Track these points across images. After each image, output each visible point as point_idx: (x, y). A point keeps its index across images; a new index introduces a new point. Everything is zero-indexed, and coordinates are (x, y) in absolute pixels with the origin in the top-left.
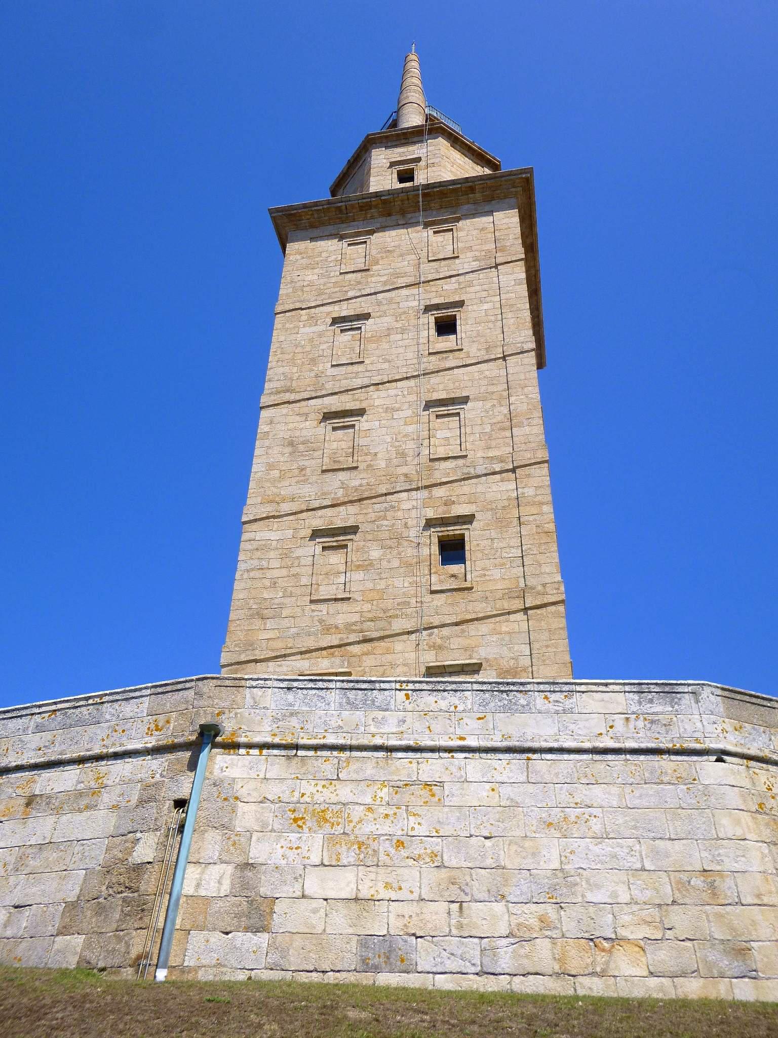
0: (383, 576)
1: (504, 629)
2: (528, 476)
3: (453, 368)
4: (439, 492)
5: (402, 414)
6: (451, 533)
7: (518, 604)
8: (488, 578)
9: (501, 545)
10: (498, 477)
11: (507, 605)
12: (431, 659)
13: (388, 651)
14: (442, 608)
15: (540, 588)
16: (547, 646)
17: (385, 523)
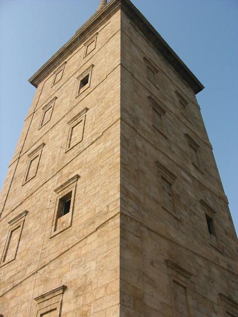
0: (32, 237)
1: (83, 252)
2: (110, 134)
3: (83, 99)
4: (65, 171)
5: (58, 137)
6: (66, 193)
7: (92, 228)
8: (80, 216)
9: (90, 188)
10: (94, 144)
11: (86, 232)
12: (40, 291)
13: (23, 292)
14: (53, 248)
15: (105, 209)
16: (106, 257)
17: (39, 203)
